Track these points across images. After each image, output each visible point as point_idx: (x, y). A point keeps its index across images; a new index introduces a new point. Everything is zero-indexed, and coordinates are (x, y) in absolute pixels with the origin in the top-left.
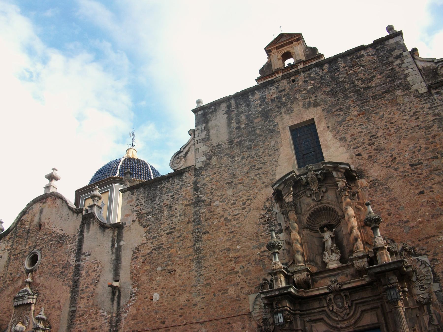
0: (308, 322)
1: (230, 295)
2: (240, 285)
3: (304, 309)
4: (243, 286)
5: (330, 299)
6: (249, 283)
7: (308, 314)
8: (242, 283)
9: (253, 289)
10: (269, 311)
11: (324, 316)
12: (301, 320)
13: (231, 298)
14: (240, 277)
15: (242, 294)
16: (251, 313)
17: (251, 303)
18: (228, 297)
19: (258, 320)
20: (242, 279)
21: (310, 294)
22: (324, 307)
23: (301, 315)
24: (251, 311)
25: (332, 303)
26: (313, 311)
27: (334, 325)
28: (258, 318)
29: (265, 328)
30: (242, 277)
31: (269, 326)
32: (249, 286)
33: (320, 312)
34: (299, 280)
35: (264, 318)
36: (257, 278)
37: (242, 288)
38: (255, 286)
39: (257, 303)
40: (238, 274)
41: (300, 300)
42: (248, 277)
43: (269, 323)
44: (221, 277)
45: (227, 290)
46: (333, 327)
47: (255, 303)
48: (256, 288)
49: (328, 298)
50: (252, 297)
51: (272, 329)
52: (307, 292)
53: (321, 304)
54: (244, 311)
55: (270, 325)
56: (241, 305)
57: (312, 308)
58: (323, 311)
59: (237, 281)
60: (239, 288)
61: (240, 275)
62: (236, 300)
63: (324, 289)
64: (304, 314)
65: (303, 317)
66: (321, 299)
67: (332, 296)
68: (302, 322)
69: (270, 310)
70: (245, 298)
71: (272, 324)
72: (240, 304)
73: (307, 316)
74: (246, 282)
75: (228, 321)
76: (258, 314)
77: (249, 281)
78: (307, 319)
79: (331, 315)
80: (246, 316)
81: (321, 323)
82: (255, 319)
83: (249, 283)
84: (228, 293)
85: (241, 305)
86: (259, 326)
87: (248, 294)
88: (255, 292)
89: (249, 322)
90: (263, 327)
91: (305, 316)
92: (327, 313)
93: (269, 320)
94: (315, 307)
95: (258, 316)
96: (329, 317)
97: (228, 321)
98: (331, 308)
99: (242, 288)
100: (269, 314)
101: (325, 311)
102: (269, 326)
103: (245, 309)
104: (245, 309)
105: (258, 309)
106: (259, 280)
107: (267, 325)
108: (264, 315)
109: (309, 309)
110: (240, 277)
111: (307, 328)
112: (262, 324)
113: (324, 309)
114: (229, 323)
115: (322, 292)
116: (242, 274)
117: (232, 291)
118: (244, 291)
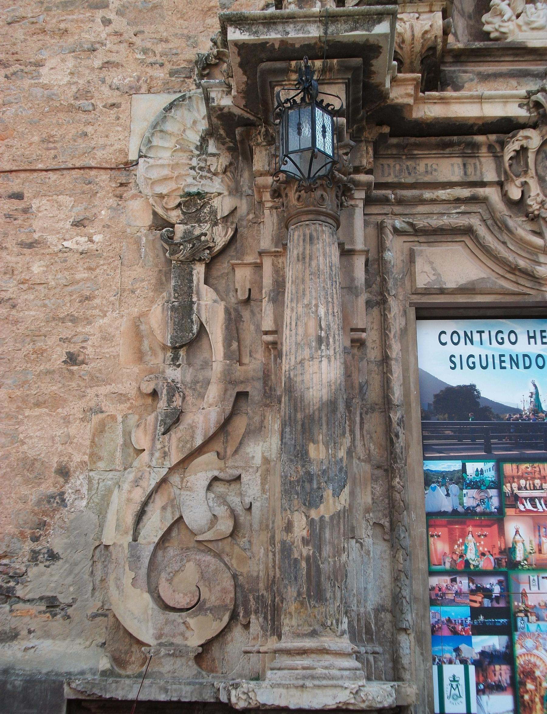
0: (397, 232)
1: (45, 87)
2: (101, 50)
3: (390, 180)
4: (114, 58)
5: (524, 150)
6: (145, 51)
7: (400, 202)
8: (115, 48)
9: (161, 74)
10: (220, 163)
11: (475, 222)
12: (366, 224)
13: (50, 98)
14: (107, 22)
15: (105, 89)
16: (129, 166)
17: (140, 127)
18: (38, 92)
19: (162, 196)
20: (116, 33)
21: (431, 110)
22: (483, 184)
23: (369, 201)
24: (133, 156)
25: (526, 172)
26: (428, 194)
27: (522, 263)
28: (163, 189)
29: (187, 233)
30: (119, 23)
31: (208, 226)
32: (142, 62)
33: (458, 201)
34: (408, 36)
35: (194, 190)
36: (189, 38)
37: (107, 64)
38: (168, 67)
39: (169, 126)
40: (100, 14)
41: (386, 130)
42: (146, 29)
43: (213, 212)
44: (21, 12)
45: (39, 64)
46: (514, 269)
47: (157, 127)
48: (172, 74)
49: (516, 146)
50: (147, 107)
51: (220, 241)
52: (424, 101)
53: (470, 170)
54: (99, 154)
55: (216, 224)
56: (90, 129)
57: (427, 179)
58: (474, 199)
59: (89, 37)
60: (97, 63)
61: (112, 16)
62: (71, 108)
63: (505, 99)
64: (385, 201)
65: (374, 210)
66: (476, 146)
67: (533, 139)
68: (371, 230)
69: (224, 160)
70: (113, 105)
71: (225, 219)
72: (88, 123)
73: (397, 209)
74: (131, 44)
75: (15, 184)
76: (166, 172)
77: (149, 45)
78: (399, 223)
79: (511, 223)
80: (104, 176)
81: (458, 248)
82: (147, 191)
83: (145, 51)
84: (39, 76)
85: (90, 129)
86: (160, 223)
87: (133, 90)
88: (167, 89)
89: (112, 202)
90: (180, 229)
91: (387, 209)
92: (491, 211)
93: (216, 202)
94: (442, 178)
95: (166, 179)
96: (499, 226)
97: (15, 184)
98: (515, 194)
99: (107, 64)
100: (217, 180)
101: (484, 201)
102: (208, 226)
103: (104, 147)
104: (104, 147)
105: (166, 154)
106: (195, 45)
107: (199, 221)
108: (190, 180)
109: (410, 180)
110: (107, 22)
111: (388, 255)
112: (174, 216)
113: (481, 191)
114: (19, 196)
115: (494, 111)
116: (120, 13)
117: (58, 73)
118: (115, 77)
